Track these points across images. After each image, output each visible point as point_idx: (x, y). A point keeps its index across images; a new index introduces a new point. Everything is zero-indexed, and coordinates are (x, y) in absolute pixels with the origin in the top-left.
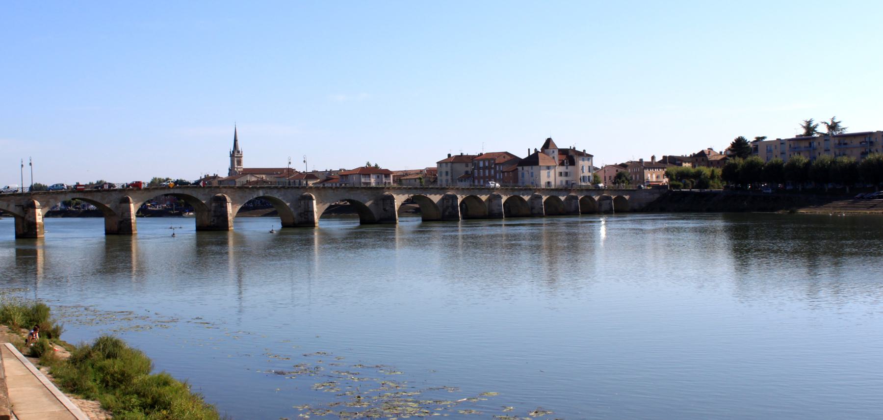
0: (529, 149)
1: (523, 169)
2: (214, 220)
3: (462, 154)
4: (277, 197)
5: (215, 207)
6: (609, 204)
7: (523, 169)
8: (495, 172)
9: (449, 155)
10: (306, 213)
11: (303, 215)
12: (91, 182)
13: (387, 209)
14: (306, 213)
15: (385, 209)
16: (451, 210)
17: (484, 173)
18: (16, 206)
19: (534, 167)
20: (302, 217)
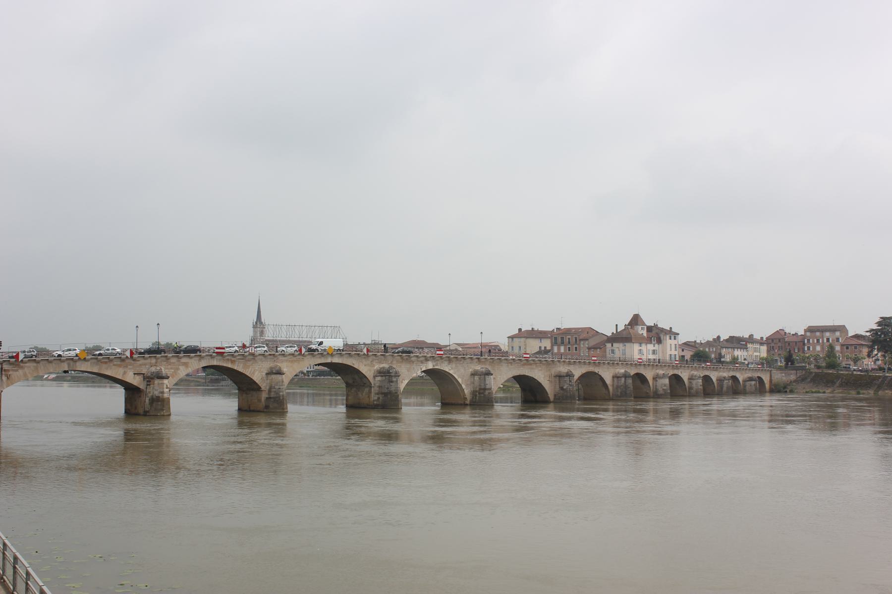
0: (617, 325)
1: (612, 346)
3: (533, 328)
4: (447, 370)
6: (754, 385)
7: (612, 346)
9: (520, 330)
10: (482, 391)
13: (565, 387)
15: (562, 388)
18: (135, 374)
19: (628, 345)
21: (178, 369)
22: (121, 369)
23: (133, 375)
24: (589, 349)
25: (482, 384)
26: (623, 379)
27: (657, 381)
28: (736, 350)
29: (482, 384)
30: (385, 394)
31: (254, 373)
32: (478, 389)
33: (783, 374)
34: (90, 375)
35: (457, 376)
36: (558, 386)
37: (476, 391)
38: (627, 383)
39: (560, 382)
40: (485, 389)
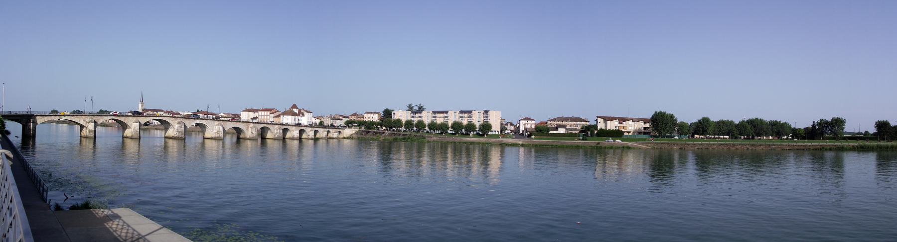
5: (178, 127)
17: (264, 117)
30: (179, 132)
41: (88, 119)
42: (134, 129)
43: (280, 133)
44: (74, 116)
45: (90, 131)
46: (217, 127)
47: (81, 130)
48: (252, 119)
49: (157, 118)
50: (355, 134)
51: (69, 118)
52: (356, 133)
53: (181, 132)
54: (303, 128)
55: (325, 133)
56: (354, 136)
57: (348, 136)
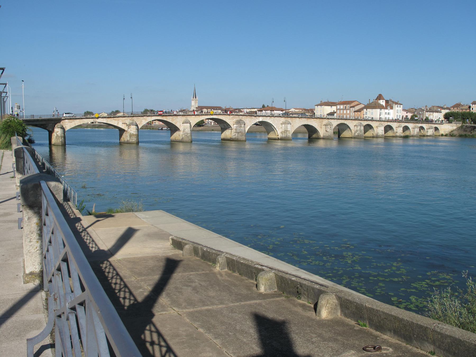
1: (367, 110)
2: (235, 135)
4: (269, 122)
5: (236, 127)
7: (367, 110)
8: (350, 112)
10: (286, 132)
11: (283, 133)
12: (146, 109)
14: (286, 132)
15: (326, 131)
16: (359, 132)
18: (122, 123)
20: (283, 134)
21: (142, 121)
22: (116, 121)
23: (122, 124)
24: (355, 112)
25: (286, 129)
26: (359, 127)
27: (378, 128)
28: (434, 113)
29: (286, 129)
30: (238, 133)
31: (176, 123)
32: (284, 131)
33: (450, 126)
34: (104, 124)
35: (274, 124)
36: (325, 130)
37: (283, 132)
38: (361, 129)
39: (326, 128)
40: (287, 131)
41: (128, 120)
42: (184, 131)
43: (361, 131)
44: (111, 117)
45: (131, 135)
46: (283, 125)
47: (121, 135)
48: (328, 114)
49: (211, 117)
50: (455, 130)
51: (105, 121)
52: (459, 129)
53: (240, 132)
54: (389, 124)
55: (417, 130)
56: (455, 133)
57: (447, 133)
